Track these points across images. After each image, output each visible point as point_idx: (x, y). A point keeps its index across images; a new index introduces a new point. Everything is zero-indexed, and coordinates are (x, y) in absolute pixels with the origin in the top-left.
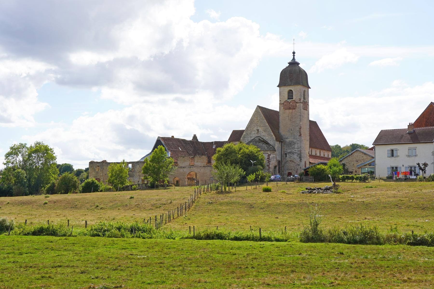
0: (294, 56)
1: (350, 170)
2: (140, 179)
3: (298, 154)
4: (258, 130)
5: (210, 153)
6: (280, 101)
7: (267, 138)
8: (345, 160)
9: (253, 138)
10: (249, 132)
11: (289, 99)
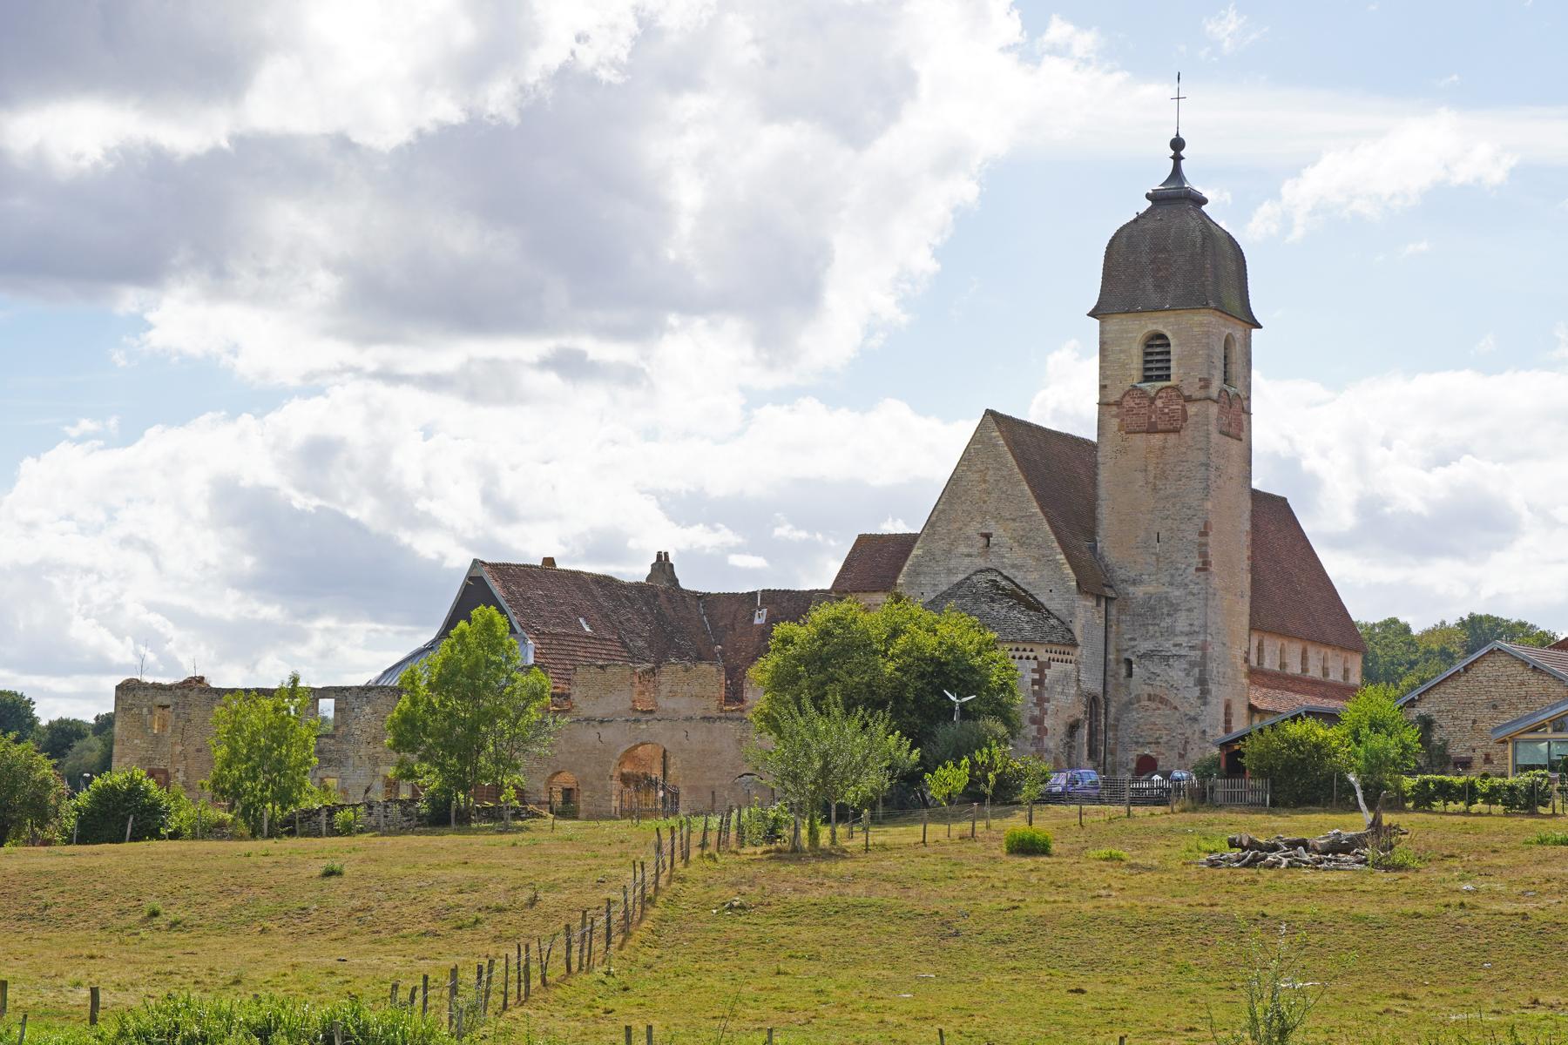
0: (1177, 159)
1: (1457, 751)
3: (1192, 664)
4: (987, 536)
5: (737, 651)
6: (1103, 387)
8: (1434, 697)
9: (961, 577)
10: (943, 545)
11: (1147, 379)
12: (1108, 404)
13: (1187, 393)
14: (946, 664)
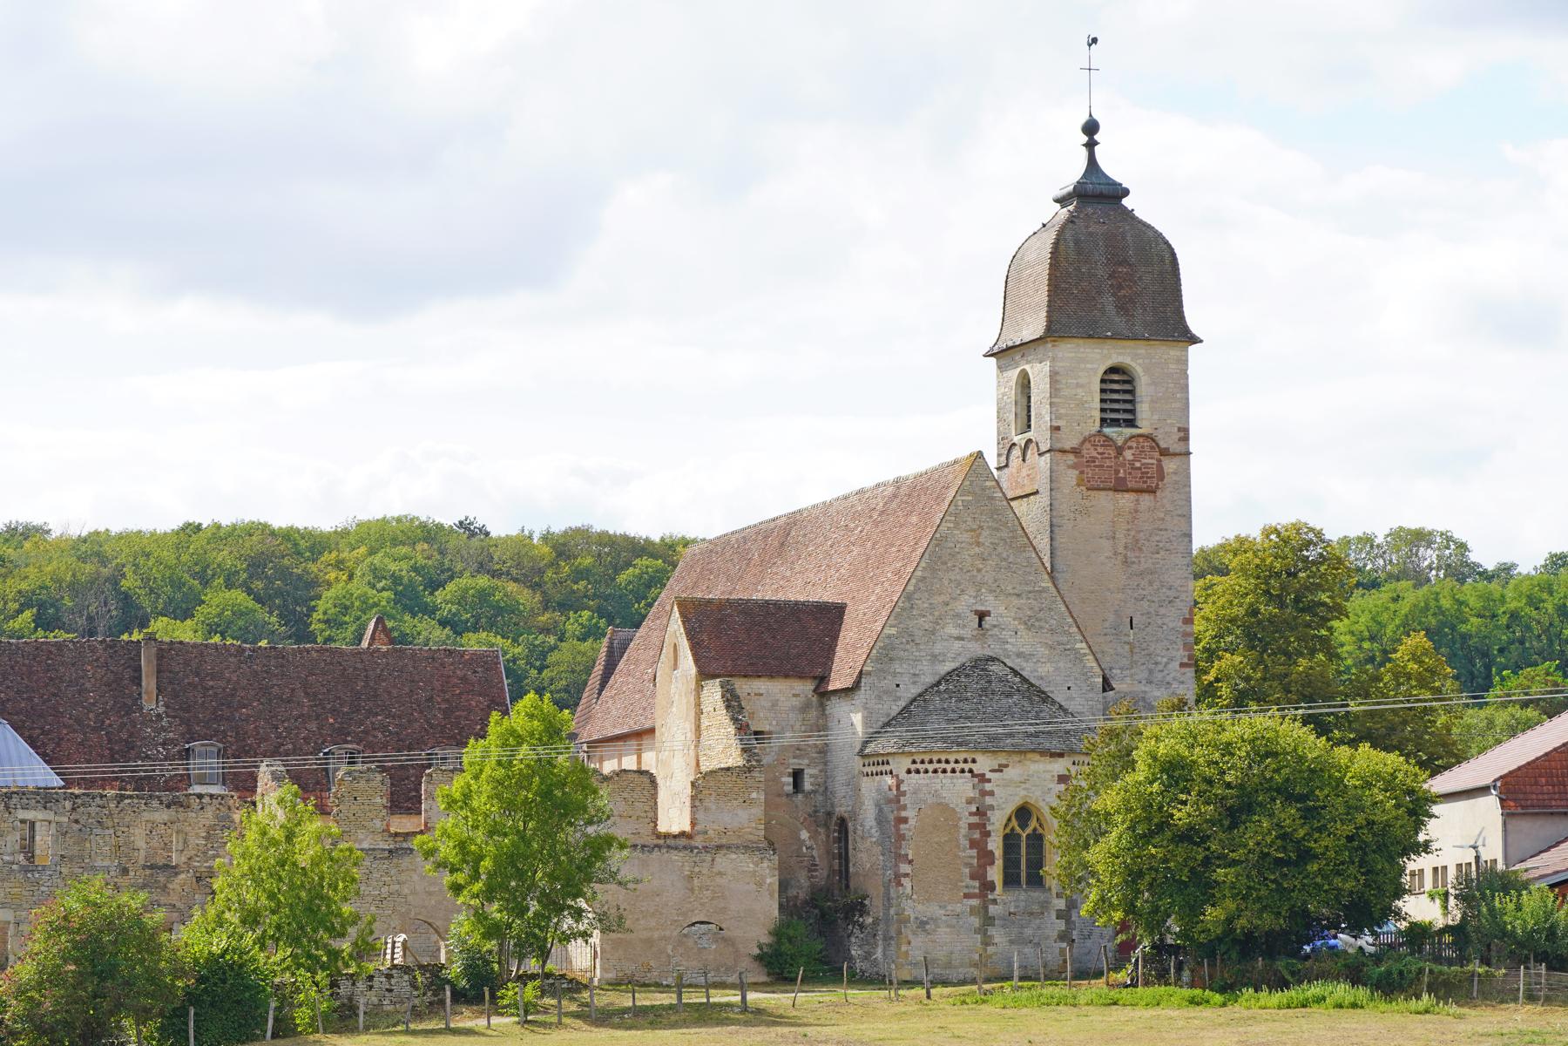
0: (1091, 145)
7: (1043, 670)
9: (949, 666)
12: (1063, 451)
13: (1163, 445)
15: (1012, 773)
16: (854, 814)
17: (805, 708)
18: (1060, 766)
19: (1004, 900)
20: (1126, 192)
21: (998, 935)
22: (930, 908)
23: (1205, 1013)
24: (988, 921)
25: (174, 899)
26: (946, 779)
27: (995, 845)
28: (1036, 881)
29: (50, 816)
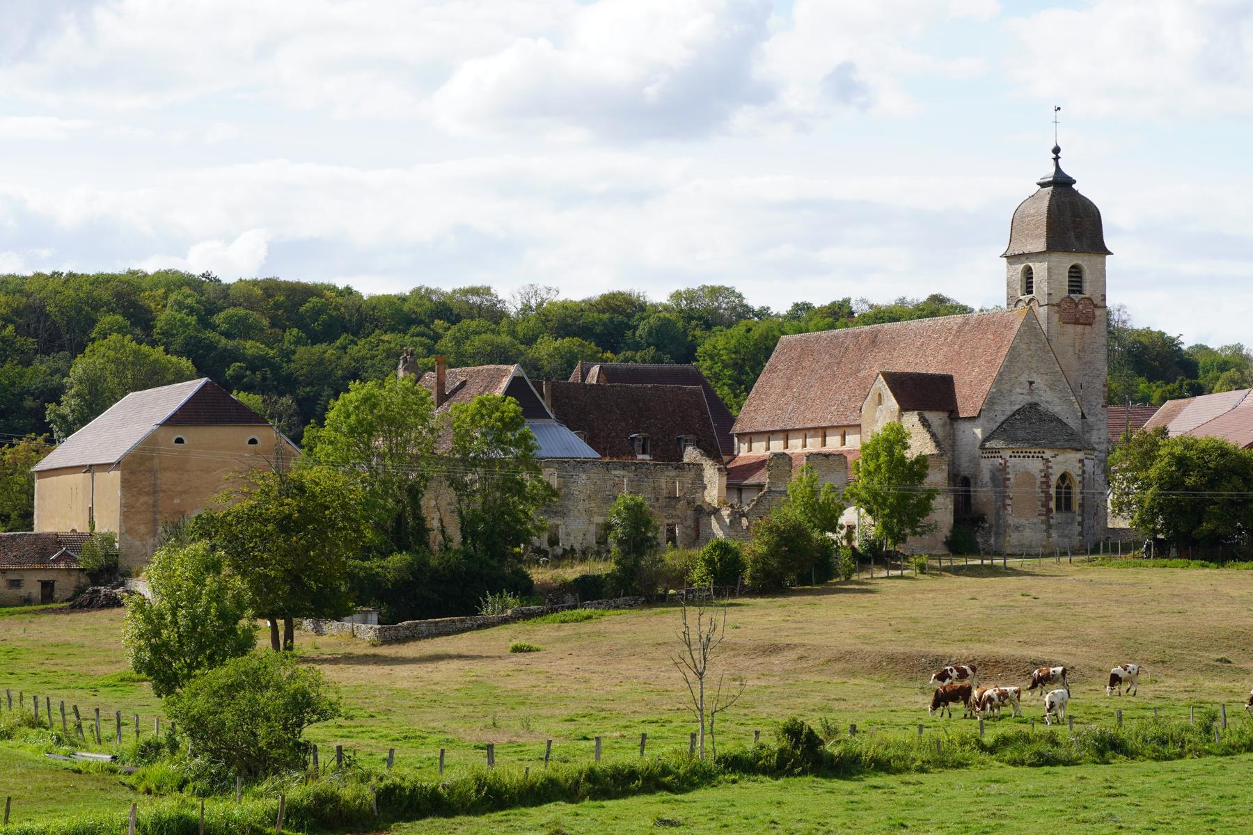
0: (1056, 159)
2: (590, 522)
3: (1101, 461)
4: (1031, 383)
9: (1017, 407)
10: (1007, 387)
14: (360, 422)
15: (1060, 458)
16: (975, 477)
17: (944, 425)
18: (1080, 455)
19: (1056, 518)
20: (1074, 182)
21: (1054, 534)
22: (1024, 524)
23: (1207, 571)
24: (1050, 526)
25: (678, 513)
26: (1030, 461)
27: (1053, 491)
28: (1068, 507)
29: (625, 473)
